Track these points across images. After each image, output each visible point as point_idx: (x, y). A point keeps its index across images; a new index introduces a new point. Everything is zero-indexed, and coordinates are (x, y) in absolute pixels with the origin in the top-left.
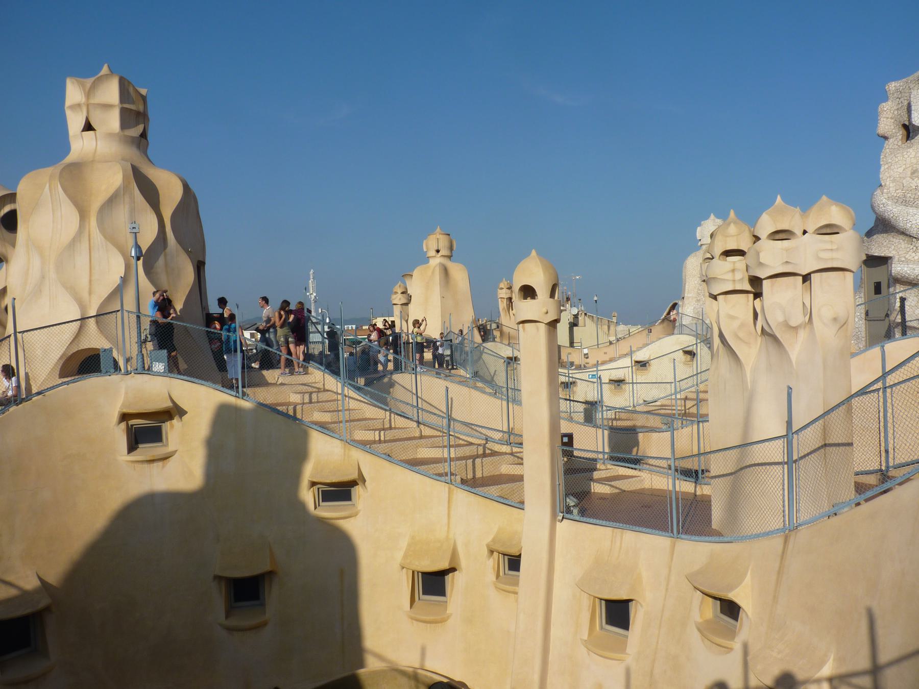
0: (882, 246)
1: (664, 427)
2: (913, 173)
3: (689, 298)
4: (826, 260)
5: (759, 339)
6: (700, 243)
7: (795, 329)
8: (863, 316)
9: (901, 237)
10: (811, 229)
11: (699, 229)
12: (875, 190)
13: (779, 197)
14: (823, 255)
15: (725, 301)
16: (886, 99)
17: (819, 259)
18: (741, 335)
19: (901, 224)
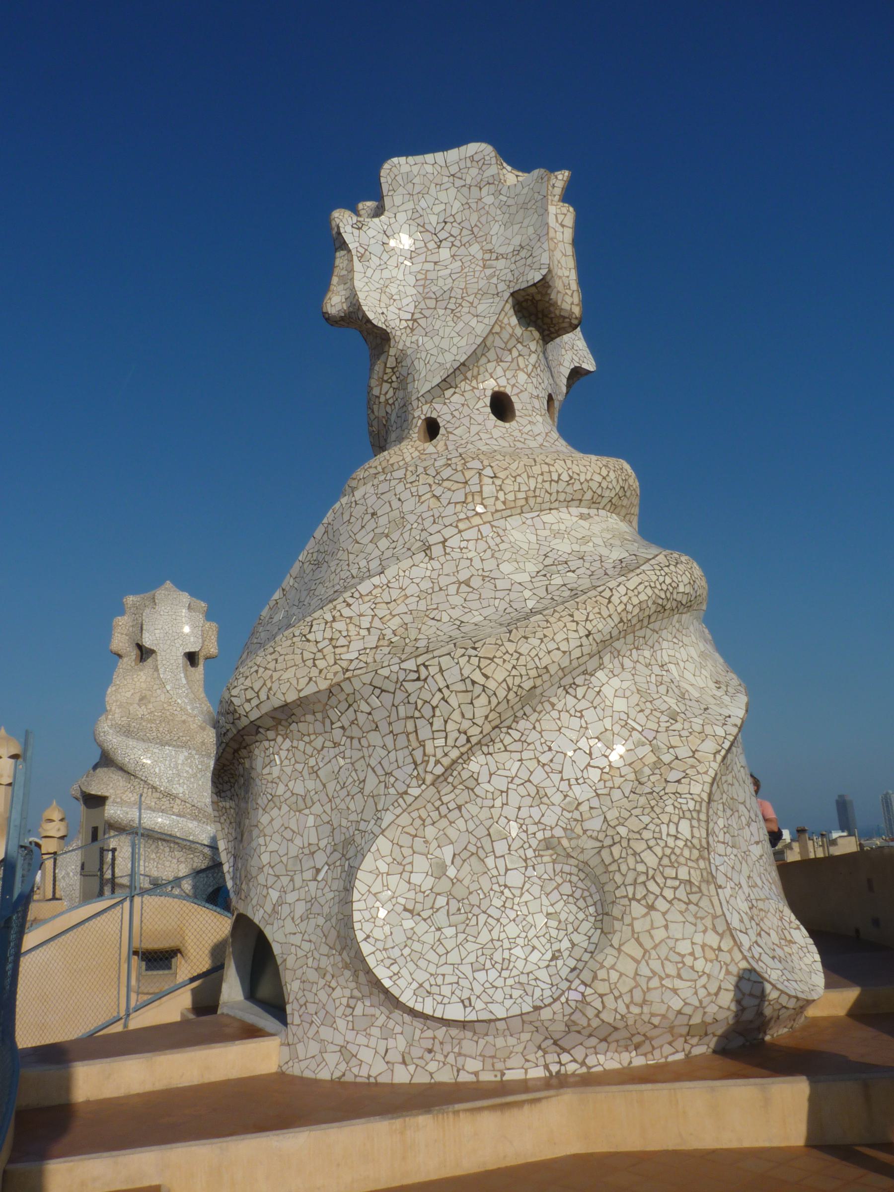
2: (141, 700)
8: (79, 869)
9: (120, 773)
16: (122, 613)
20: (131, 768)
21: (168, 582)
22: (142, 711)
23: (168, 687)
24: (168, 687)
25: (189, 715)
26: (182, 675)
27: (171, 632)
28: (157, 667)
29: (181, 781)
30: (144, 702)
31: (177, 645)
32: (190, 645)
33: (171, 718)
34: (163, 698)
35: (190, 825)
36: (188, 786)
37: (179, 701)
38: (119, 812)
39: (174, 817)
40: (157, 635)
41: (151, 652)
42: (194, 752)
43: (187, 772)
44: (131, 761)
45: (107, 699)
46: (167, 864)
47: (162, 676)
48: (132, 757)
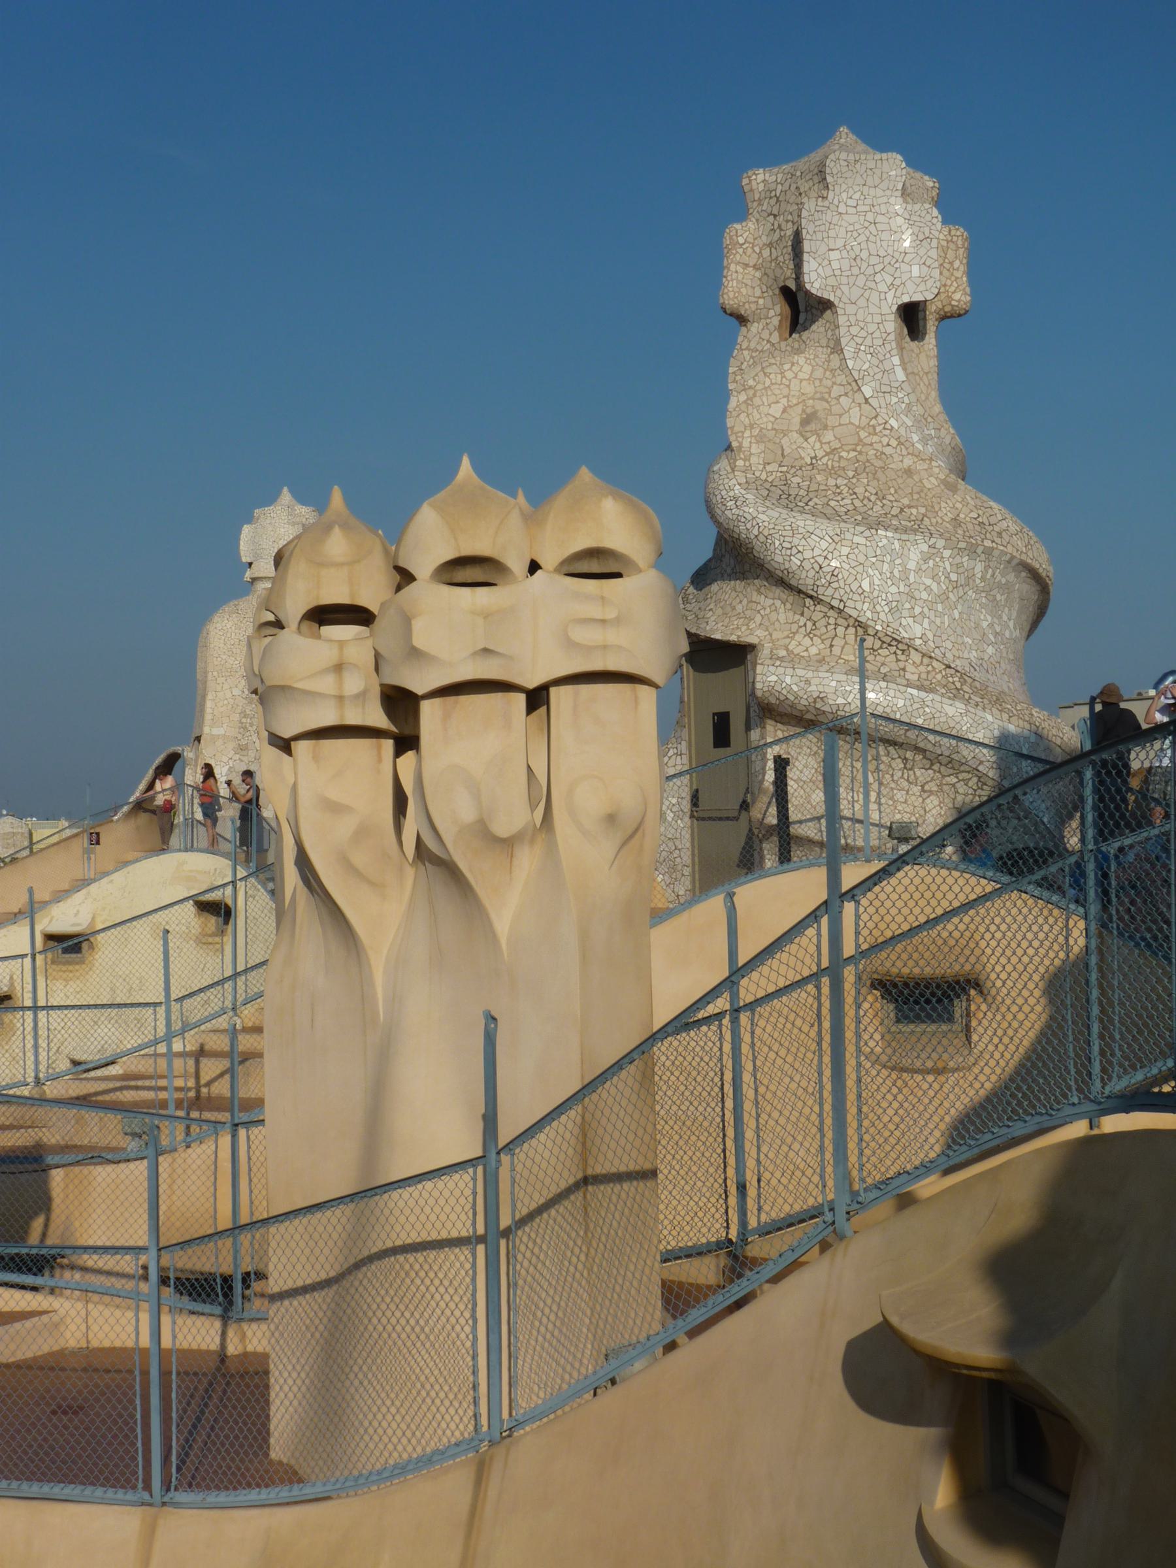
0: (736, 614)
1: (133, 1145)
2: (806, 421)
3: (214, 738)
4: (588, 649)
5: (410, 872)
6: (248, 575)
7: (507, 844)
8: (686, 805)
9: (778, 591)
10: (550, 559)
11: (246, 530)
12: (715, 460)
13: (466, 462)
14: (581, 635)
15: (316, 758)
16: (742, 215)
17: (571, 645)
18: (360, 859)
19: (777, 559)
20: (806, 580)
21: (844, 129)
22: (810, 448)
23: (867, 391)
24: (867, 391)
25: (917, 455)
26: (896, 360)
27: (864, 255)
28: (838, 341)
29: (917, 610)
30: (813, 426)
31: (882, 287)
32: (910, 287)
33: (878, 463)
34: (855, 416)
35: (950, 711)
36: (932, 622)
37: (893, 422)
38: (788, 680)
39: (915, 692)
40: (835, 265)
41: (824, 305)
42: (941, 543)
43: (928, 588)
44: (807, 565)
45: (730, 422)
46: (900, 796)
47: (850, 363)
48: (808, 554)
